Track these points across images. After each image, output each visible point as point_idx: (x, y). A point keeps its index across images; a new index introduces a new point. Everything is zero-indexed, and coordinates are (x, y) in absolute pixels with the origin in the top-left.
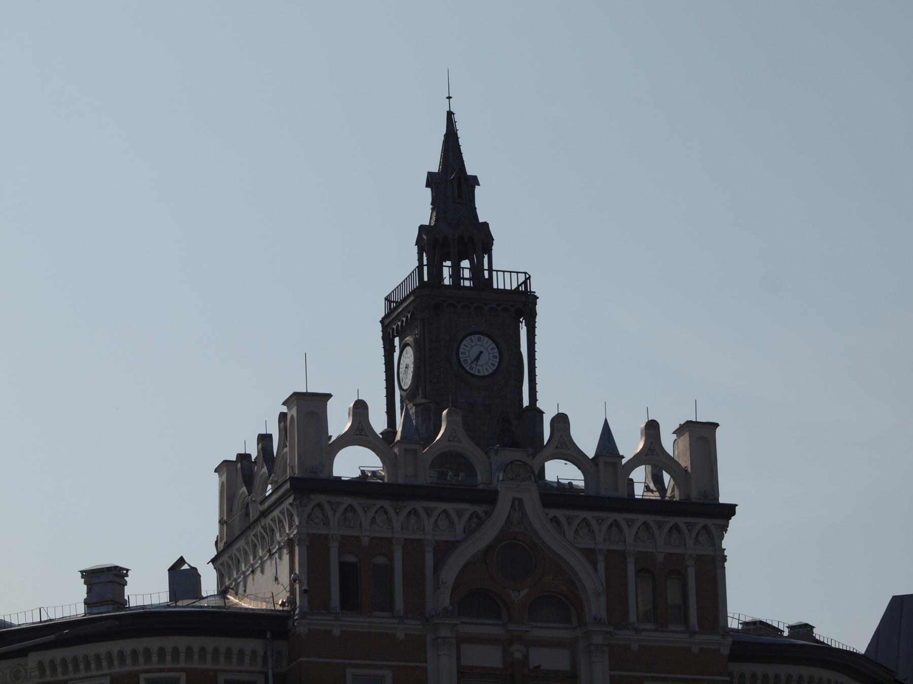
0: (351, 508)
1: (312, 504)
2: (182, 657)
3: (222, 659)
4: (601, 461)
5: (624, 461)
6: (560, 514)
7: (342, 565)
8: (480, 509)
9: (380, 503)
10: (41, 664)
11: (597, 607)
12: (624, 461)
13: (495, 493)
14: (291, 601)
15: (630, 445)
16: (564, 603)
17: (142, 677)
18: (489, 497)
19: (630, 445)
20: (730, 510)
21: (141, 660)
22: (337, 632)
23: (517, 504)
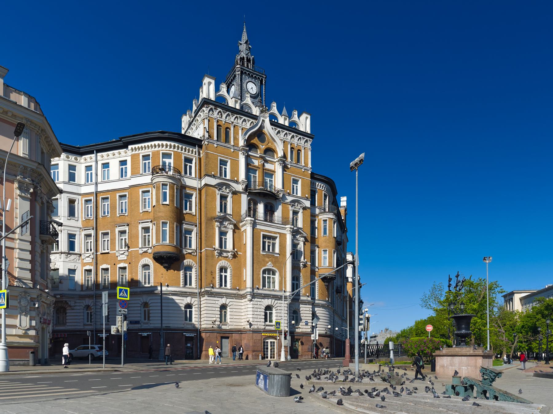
10: (132, 148)
14: (204, 136)
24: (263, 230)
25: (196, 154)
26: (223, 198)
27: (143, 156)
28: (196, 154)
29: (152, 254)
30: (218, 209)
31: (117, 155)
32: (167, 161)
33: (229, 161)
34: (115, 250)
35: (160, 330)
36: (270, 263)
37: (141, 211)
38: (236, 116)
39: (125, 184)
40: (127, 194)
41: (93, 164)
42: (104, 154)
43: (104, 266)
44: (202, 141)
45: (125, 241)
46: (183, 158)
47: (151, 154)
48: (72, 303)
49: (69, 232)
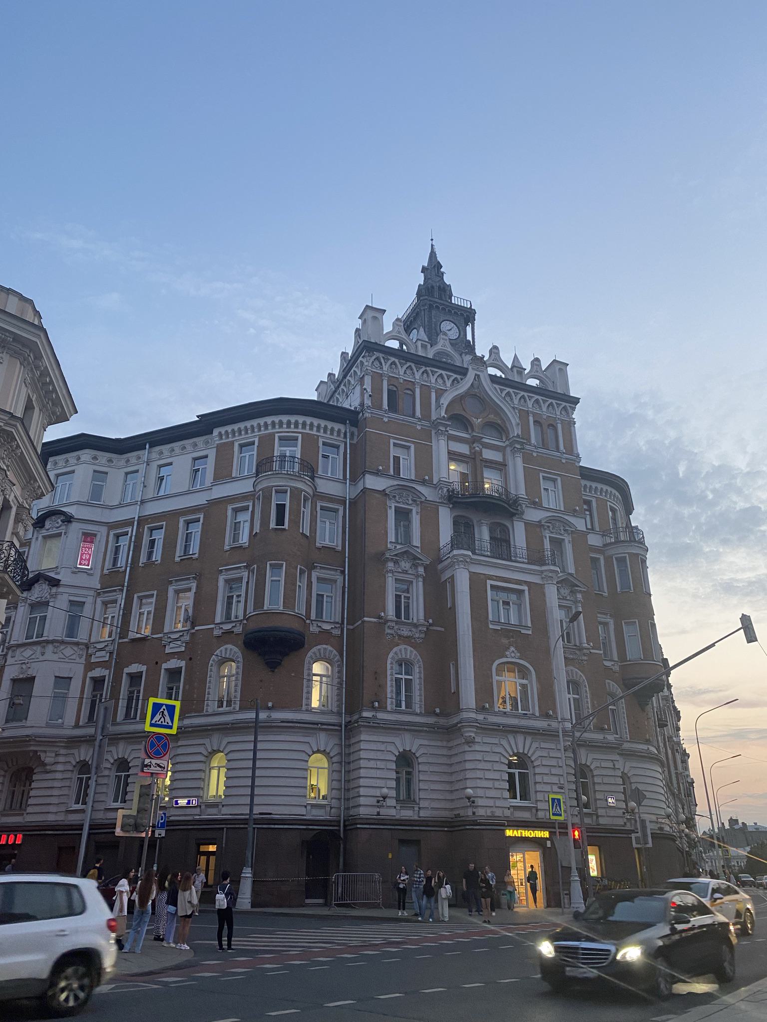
0: (394, 363)
1: (374, 357)
2: (300, 426)
3: (322, 431)
4: (515, 370)
5: (526, 372)
6: (497, 387)
7: (389, 390)
8: (459, 377)
9: (409, 364)
10: (220, 433)
11: (517, 431)
12: (526, 372)
13: (467, 369)
14: (362, 404)
15: (527, 366)
16: (499, 428)
17: (277, 435)
18: (463, 372)
19: (527, 366)
20: (576, 401)
21: (277, 427)
22: (386, 420)
23: (477, 376)
24: (491, 577)
25: (345, 437)
26: (403, 515)
27: (241, 446)
28: (345, 437)
29: (242, 638)
30: (391, 537)
31: (189, 448)
32: (288, 451)
33: (413, 446)
34: (161, 631)
35: (245, 821)
36: (512, 649)
37: (227, 548)
38: (424, 369)
39: (200, 499)
40: (202, 516)
41: (142, 468)
42: (165, 448)
43: (134, 668)
44: (358, 413)
45: (186, 610)
46: (320, 444)
47: (256, 440)
48: (48, 758)
49: (72, 598)
